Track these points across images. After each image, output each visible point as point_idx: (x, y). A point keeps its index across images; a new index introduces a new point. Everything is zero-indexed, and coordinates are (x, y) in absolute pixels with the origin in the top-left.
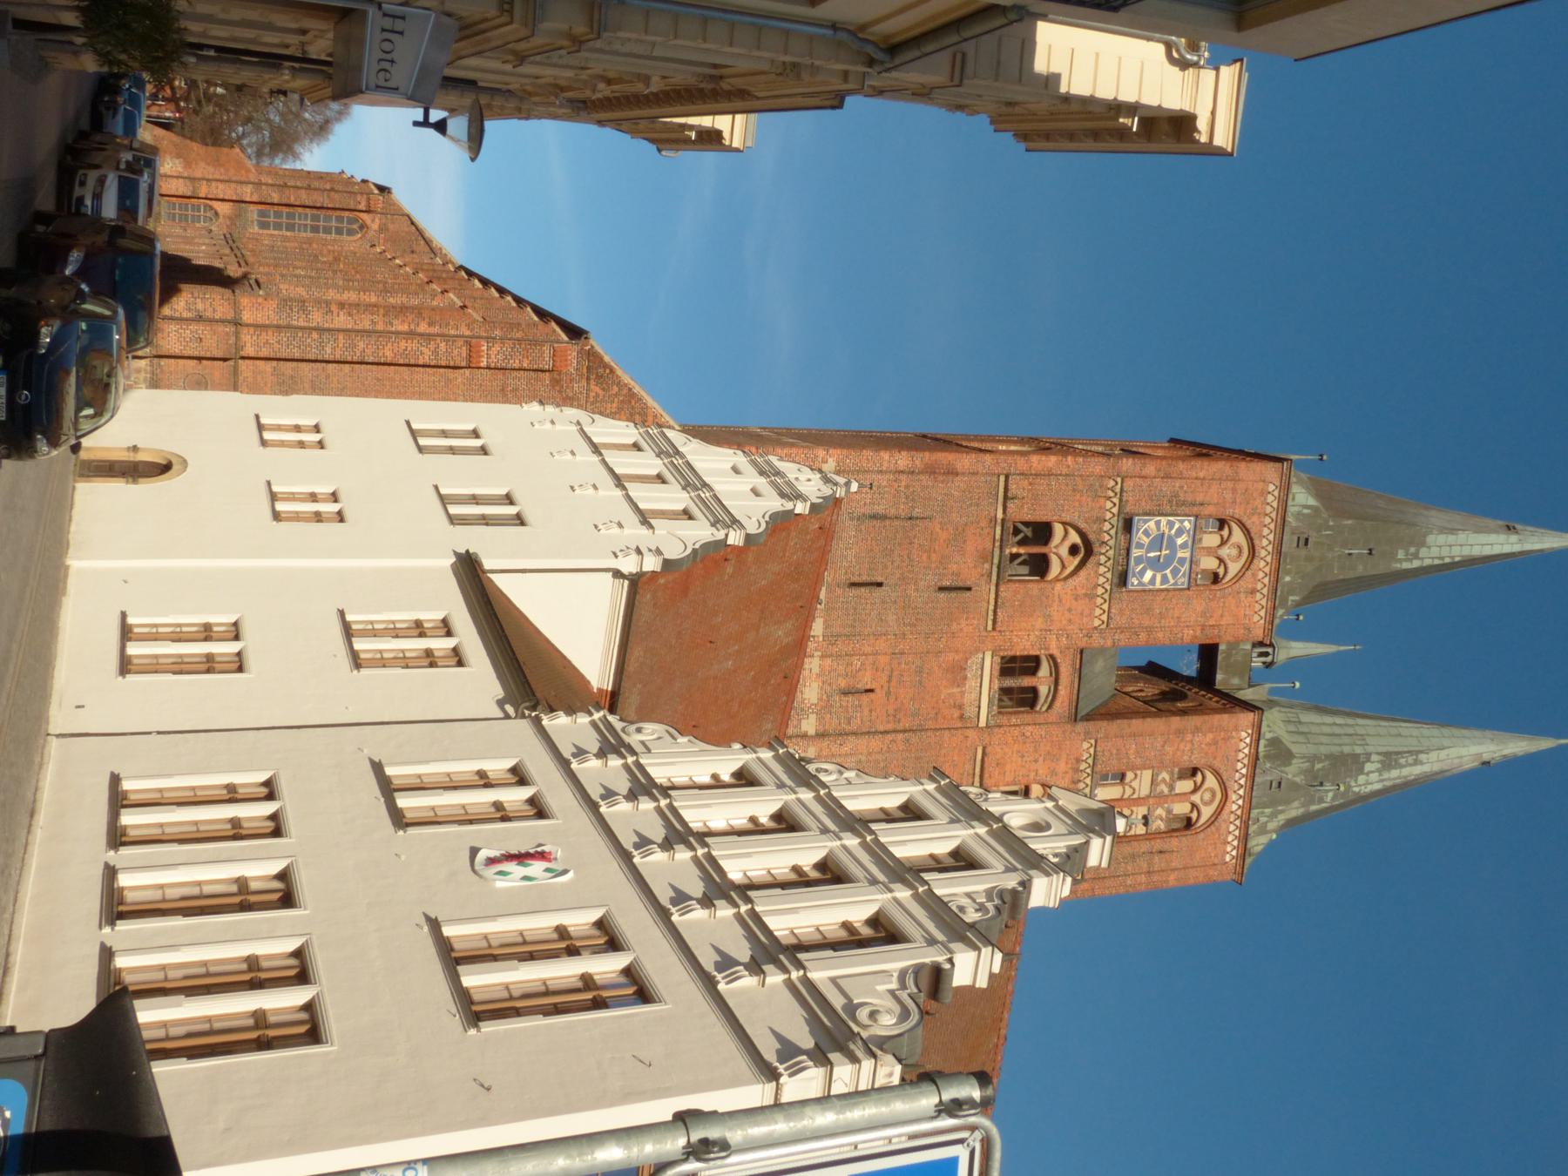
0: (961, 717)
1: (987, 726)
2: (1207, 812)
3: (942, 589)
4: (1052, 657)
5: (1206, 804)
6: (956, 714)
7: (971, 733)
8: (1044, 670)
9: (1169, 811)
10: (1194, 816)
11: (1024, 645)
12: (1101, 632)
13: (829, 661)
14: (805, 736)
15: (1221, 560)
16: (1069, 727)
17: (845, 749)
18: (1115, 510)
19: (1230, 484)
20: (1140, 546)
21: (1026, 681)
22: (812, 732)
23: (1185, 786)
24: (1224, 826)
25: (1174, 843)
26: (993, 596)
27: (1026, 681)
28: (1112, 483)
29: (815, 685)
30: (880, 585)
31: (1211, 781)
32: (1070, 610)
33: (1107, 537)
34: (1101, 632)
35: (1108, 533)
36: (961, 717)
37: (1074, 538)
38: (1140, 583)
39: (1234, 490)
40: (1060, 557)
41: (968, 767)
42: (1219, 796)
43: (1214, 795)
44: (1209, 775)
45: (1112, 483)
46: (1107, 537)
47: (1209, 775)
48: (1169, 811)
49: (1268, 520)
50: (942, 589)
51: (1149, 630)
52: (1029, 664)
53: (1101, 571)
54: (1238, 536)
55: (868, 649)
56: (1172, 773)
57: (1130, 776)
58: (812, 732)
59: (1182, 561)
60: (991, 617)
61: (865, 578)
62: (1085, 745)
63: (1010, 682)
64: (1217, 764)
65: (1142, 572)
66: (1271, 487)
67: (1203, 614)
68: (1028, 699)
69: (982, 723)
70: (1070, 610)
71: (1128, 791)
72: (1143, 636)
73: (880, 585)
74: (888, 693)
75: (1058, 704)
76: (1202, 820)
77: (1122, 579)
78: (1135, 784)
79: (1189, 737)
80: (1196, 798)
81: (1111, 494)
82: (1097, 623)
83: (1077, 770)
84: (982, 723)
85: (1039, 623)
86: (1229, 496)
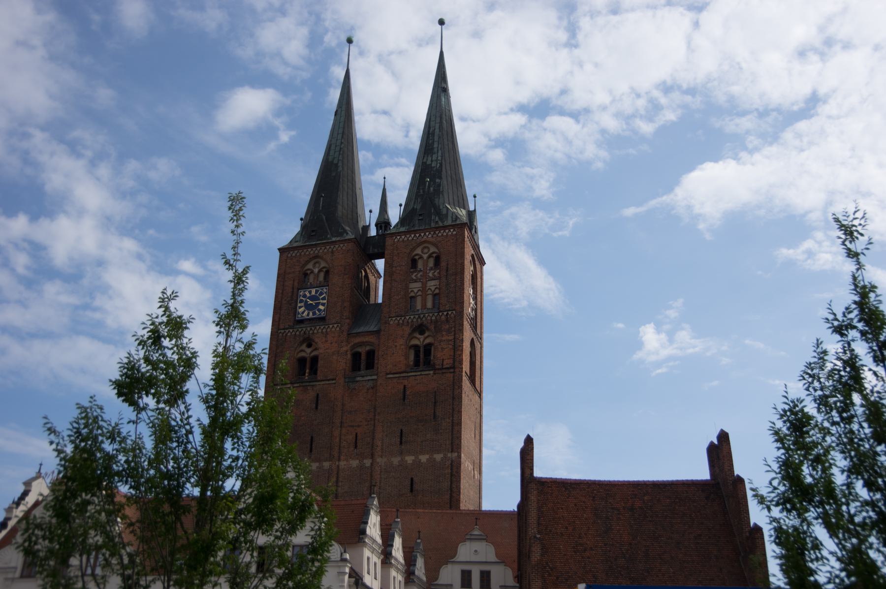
0: (372, 388)
3: (317, 408)
4: (353, 347)
7: (379, 383)
8: (359, 350)
9: (431, 269)
10: (434, 255)
11: (342, 363)
13: (342, 457)
14: (372, 464)
16: (382, 333)
17: (379, 443)
21: (363, 357)
22: (370, 461)
23: (420, 265)
25: (443, 264)
27: (363, 357)
29: (351, 462)
30: (312, 438)
31: (418, 251)
37: (304, 347)
41: (395, 380)
43: (425, 247)
44: (415, 253)
47: (415, 253)
48: (431, 269)
50: (317, 408)
52: (356, 356)
54: (310, 266)
55: (338, 439)
57: (412, 294)
58: (370, 461)
61: (308, 445)
63: (363, 365)
65: (319, 310)
68: (371, 354)
69: (375, 377)
71: (420, 293)
73: (312, 438)
74: (359, 426)
77: (322, 319)
78: (416, 290)
80: (425, 256)
83: (403, 324)
84: (375, 377)
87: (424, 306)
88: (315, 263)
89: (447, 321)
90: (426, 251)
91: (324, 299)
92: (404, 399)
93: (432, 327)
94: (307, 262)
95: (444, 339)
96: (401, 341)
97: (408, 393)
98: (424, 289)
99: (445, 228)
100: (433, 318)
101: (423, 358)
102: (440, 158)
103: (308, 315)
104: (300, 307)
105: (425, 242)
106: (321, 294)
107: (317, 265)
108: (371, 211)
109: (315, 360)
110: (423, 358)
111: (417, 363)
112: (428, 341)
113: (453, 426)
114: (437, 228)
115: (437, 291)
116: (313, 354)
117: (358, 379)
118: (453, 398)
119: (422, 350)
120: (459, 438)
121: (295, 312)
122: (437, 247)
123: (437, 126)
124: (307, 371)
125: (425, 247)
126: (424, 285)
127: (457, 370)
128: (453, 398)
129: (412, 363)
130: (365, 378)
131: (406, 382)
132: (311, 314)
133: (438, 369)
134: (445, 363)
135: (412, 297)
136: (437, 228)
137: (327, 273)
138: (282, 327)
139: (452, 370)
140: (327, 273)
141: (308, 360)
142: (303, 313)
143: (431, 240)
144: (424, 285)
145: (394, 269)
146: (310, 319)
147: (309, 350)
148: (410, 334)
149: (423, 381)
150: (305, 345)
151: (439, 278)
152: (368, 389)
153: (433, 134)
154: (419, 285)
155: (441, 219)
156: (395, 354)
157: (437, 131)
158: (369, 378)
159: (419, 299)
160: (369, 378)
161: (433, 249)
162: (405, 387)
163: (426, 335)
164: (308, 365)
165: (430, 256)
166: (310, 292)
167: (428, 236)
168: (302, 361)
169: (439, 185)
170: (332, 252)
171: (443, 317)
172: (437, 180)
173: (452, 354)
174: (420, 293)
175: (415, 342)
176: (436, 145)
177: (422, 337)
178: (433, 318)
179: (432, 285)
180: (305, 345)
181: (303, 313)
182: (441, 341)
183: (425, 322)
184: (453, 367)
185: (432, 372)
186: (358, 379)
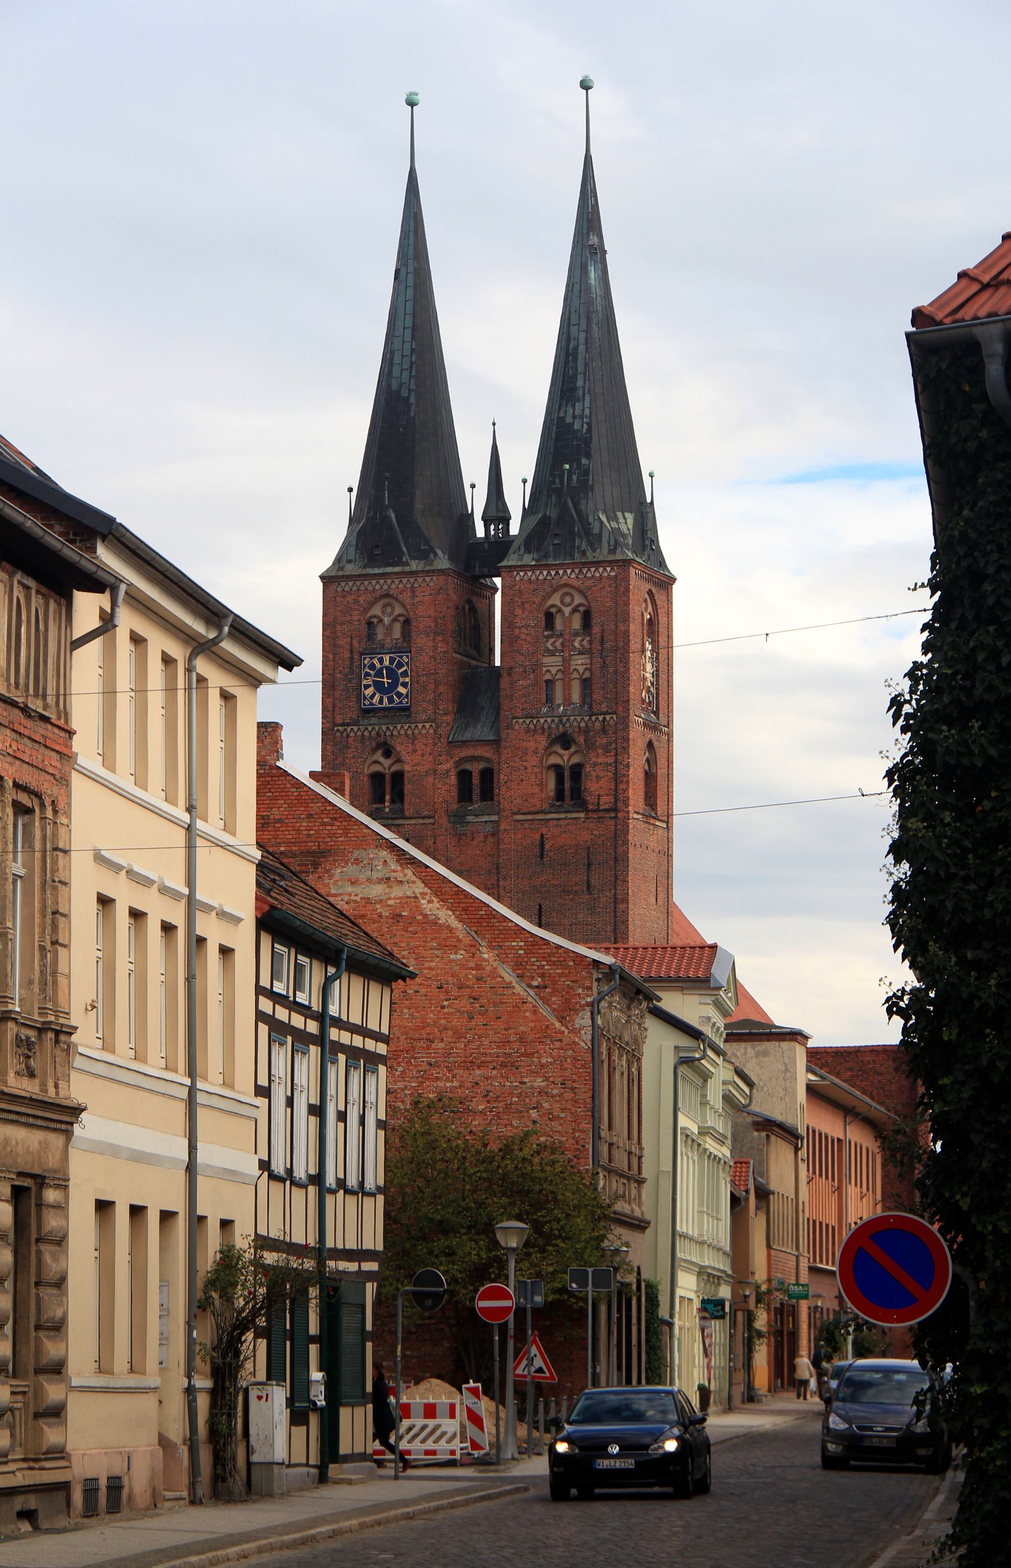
0: (493, 835)
1: (498, 814)
2: (578, 599)
5: (573, 600)
6: (490, 839)
7: (502, 827)
8: (468, 766)
10: (582, 609)
12: (437, 727)
15: (395, 620)
18: (355, 728)
19: (338, 628)
20: (381, 702)
21: (476, 781)
24: (588, 583)
25: (596, 630)
26: (413, 821)
27: (476, 781)
28: (338, 734)
32: (423, 755)
33: (374, 732)
34: (437, 727)
35: (374, 726)
36: (493, 835)
38: (407, 696)
39: (342, 624)
40: (392, 765)
41: (527, 825)
42: (566, 590)
43: (567, 594)
45: (338, 734)
46: (374, 732)
49: (362, 588)
51: (437, 683)
53: (398, 731)
56: (548, 637)
57: (548, 677)
59: (392, 660)
60: (427, 821)
62: (517, 727)
64: (537, 600)
65: (399, 695)
66: (339, 589)
67: (427, 635)
68: (488, 776)
69: (495, 818)
70: (423, 755)
71: (560, 676)
72: (442, 689)
75: (488, 755)
76: (585, 602)
78: (554, 670)
79: (517, 631)
80: (567, 611)
81: (345, 734)
82: (431, 731)
83: (535, 730)
84: (495, 818)
85: (430, 780)
86: (346, 627)
87: (567, 700)
88: (385, 606)
89: (604, 730)
90: (568, 599)
91: (405, 674)
92: (542, 856)
93: (581, 740)
94: (371, 604)
95: (600, 761)
96: (533, 761)
97: (547, 846)
98: (566, 669)
99: (597, 564)
100: (582, 725)
101: (570, 788)
102: (587, 412)
103: (381, 702)
104: (367, 687)
105: (566, 585)
106: (400, 665)
107: (389, 610)
108: (473, 486)
109: (398, 777)
110: (570, 788)
111: (560, 795)
112: (575, 760)
113: (615, 903)
114: (584, 564)
115: (587, 675)
116: (394, 769)
117: (470, 818)
118: (616, 860)
119: (567, 774)
120: (626, 922)
121: (360, 697)
122: (586, 597)
123: (582, 336)
124: (388, 798)
125: (567, 594)
126: (566, 662)
127: (620, 815)
128: (616, 860)
129: (552, 794)
130: (480, 820)
131: (544, 830)
132: (385, 700)
133: (593, 811)
134: (602, 802)
135: (547, 681)
136: (584, 564)
137: (407, 623)
138: (339, 719)
139: (613, 815)
140: (407, 623)
141: (388, 778)
142: (373, 696)
143: (577, 583)
144: (566, 662)
145: (517, 631)
146: (385, 709)
147: (387, 762)
148: (546, 749)
149: (571, 830)
150: (380, 752)
151: (590, 652)
152: (486, 837)
153: (575, 355)
154: (557, 660)
155: (590, 544)
156: (526, 779)
157: (582, 348)
158: (486, 818)
159: (559, 687)
160: (486, 818)
161: (578, 599)
162: (542, 836)
163: (573, 749)
164: (388, 788)
165: (575, 610)
166: (381, 660)
167: (571, 576)
168: (377, 778)
169: (587, 472)
170: (413, 590)
171: (597, 724)
172: (584, 461)
173: (613, 787)
174: (560, 676)
175: (554, 760)
176: (580, 383)
177: (566, 754)
178: (582, 725)
179: (579, 663)
180: (380, 752)
181: (373, 696)
182: (595, 764)
183: (570, 731)
184: (615, 810)
185: (582, 815)
186: (470, 818)
